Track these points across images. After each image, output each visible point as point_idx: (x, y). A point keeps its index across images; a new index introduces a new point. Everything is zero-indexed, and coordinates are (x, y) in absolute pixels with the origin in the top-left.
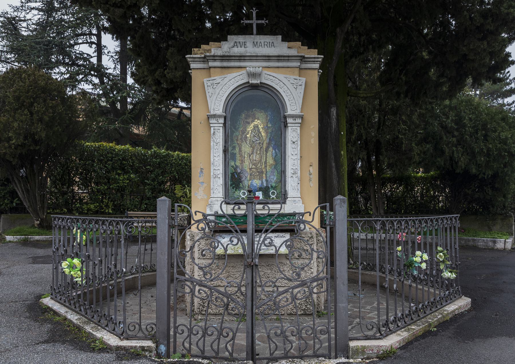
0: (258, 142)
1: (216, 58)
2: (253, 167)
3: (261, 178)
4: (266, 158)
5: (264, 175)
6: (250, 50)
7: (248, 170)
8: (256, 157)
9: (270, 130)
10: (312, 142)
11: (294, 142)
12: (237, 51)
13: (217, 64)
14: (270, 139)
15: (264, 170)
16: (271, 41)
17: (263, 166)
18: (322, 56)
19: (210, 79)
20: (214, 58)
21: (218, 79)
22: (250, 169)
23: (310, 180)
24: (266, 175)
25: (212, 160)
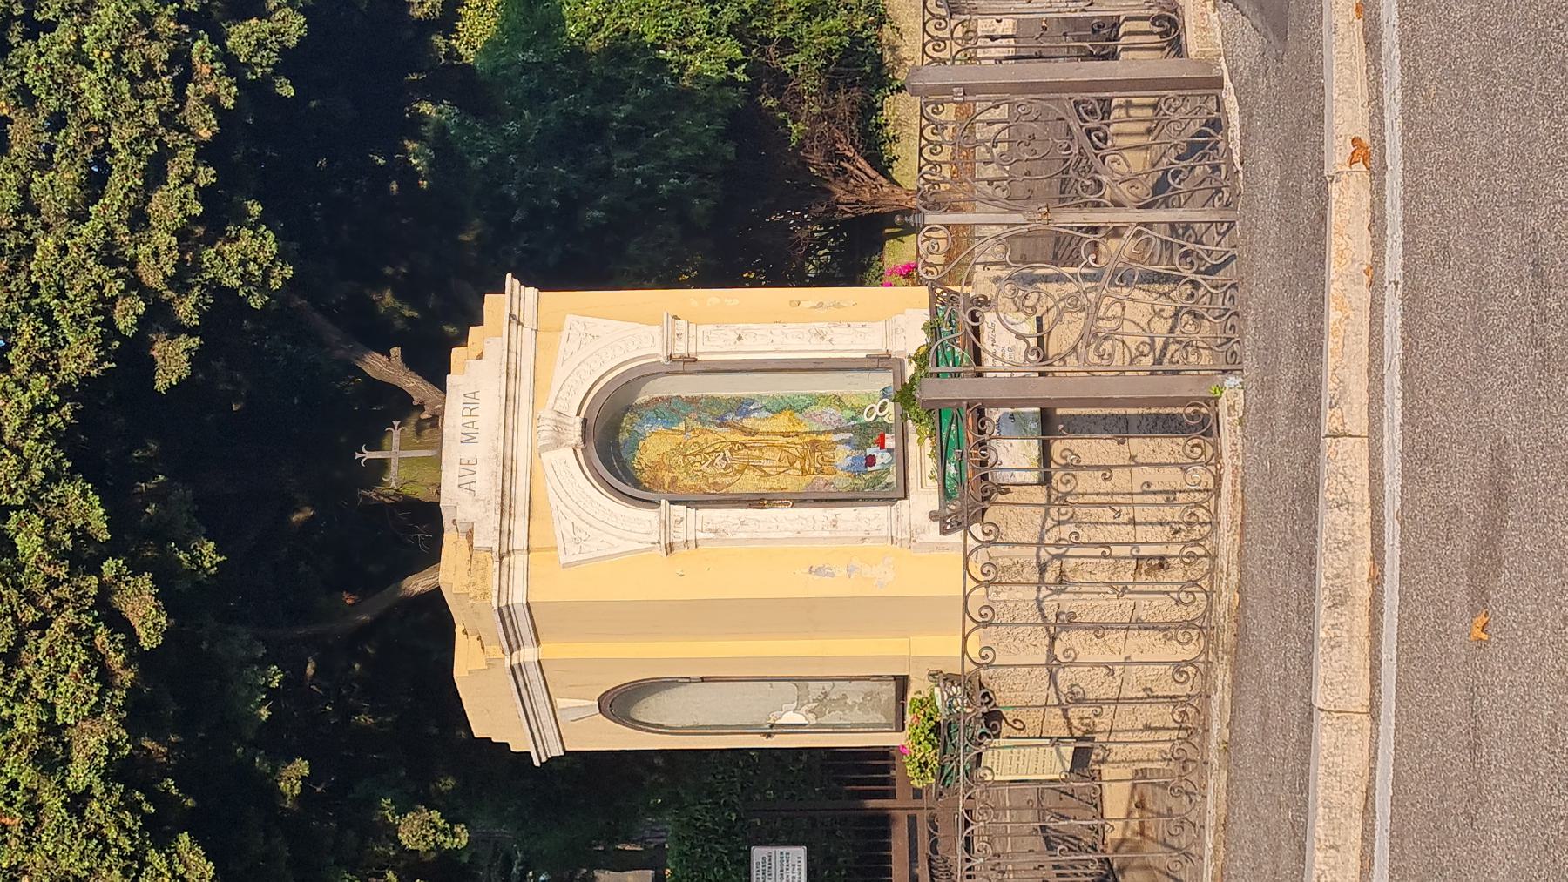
0: (728, 454)
1: (505, 529)
2: (797, 465)
3: (832, 446)
4: (774, 434)
5: (822, 438)
6: (484, 449)
7: (809, 478)
8: (770, 459)
9: (696, 425)
10: (736, 302)
11: (740, 338)
12: (486, 481)
13: (519, 527)
14: (720, 426)
15: (807, 439)
16: (463, 400)
17: (796, 440)
18: (509, 276)
19: (561, 547)
20: (505, 533)
21: (563, 527)
22: (804, 472)
23: (838, 306)
24: (819, 433)
25: (787, 534)
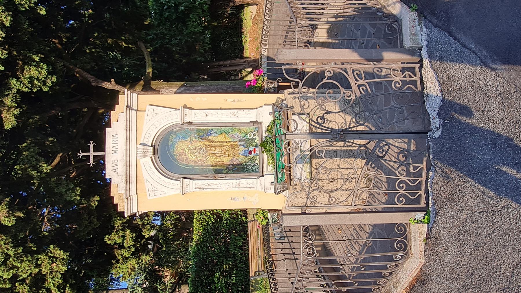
1: (128, 188)
2: (227, 153)
4: (220, 142)
5: (235, 143)
6: (120, 156)
7: (230, 158)
11: (207, 115)
12: (121, 168)
16: (112, 137)
20: (128, 190)
24: (234, 142)
